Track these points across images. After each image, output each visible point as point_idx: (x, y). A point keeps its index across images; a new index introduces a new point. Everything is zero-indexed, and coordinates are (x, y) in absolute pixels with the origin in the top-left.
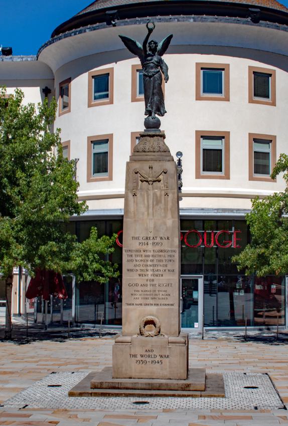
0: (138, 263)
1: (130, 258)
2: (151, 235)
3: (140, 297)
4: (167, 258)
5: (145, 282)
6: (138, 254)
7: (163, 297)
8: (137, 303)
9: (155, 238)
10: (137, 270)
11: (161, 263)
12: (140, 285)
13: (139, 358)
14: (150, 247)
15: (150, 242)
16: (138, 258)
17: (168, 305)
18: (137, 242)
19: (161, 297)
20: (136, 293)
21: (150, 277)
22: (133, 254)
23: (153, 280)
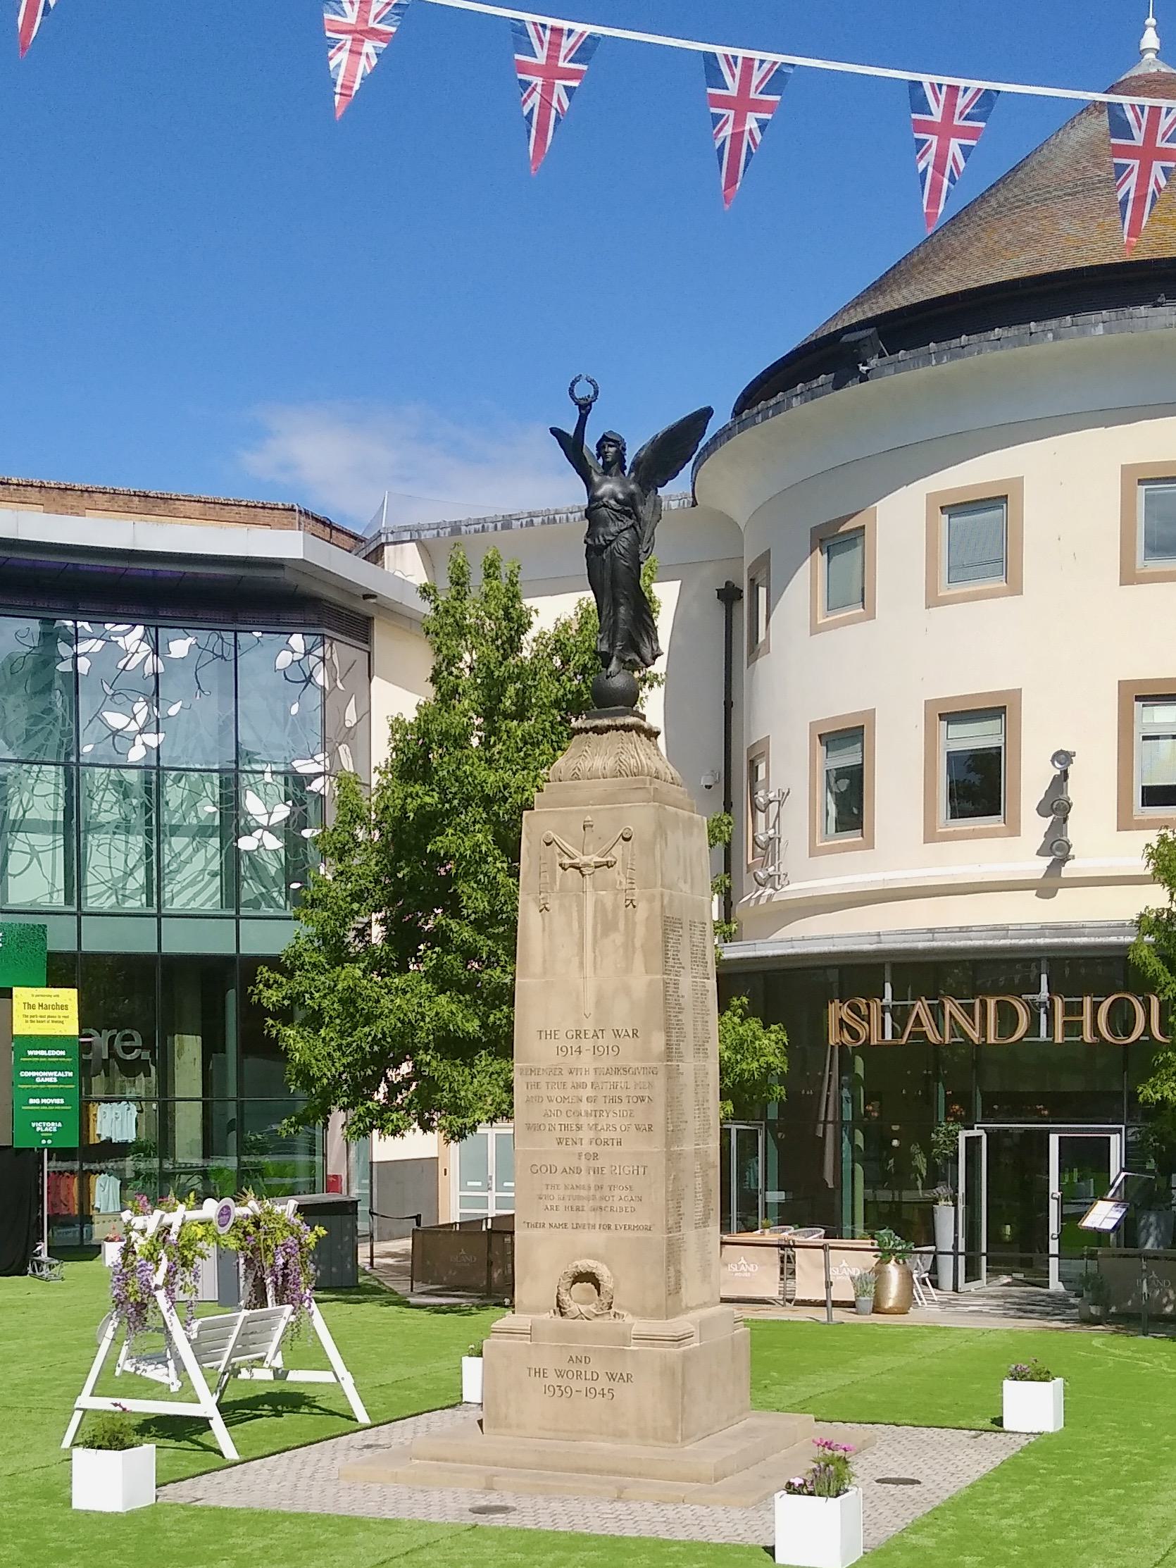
0: (554, 1106)
1: (534, 1092)
2: (589, 1026)
3: (561, 1204)
4: (631, 1093)
5: (574, 1162)
6: (557, 1079)
7: (623, 1204)
8: (555, 1221)
9: (600, 1035)
10: (552, 1128)
11: (617, 1107)
12: (560, 1169)
13: (552, 1379)
14: (586, 1061)
15: (587, 1044)
16: (556, 1093)
17: (638, 1228)
18: (553, 1043)
19: (617, 1204)
20: (550, 1192)
21: (586, 1148)
22: (543, 1079)
23: (596, 1156)
